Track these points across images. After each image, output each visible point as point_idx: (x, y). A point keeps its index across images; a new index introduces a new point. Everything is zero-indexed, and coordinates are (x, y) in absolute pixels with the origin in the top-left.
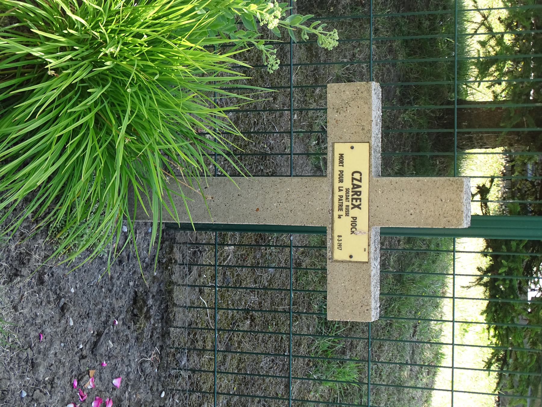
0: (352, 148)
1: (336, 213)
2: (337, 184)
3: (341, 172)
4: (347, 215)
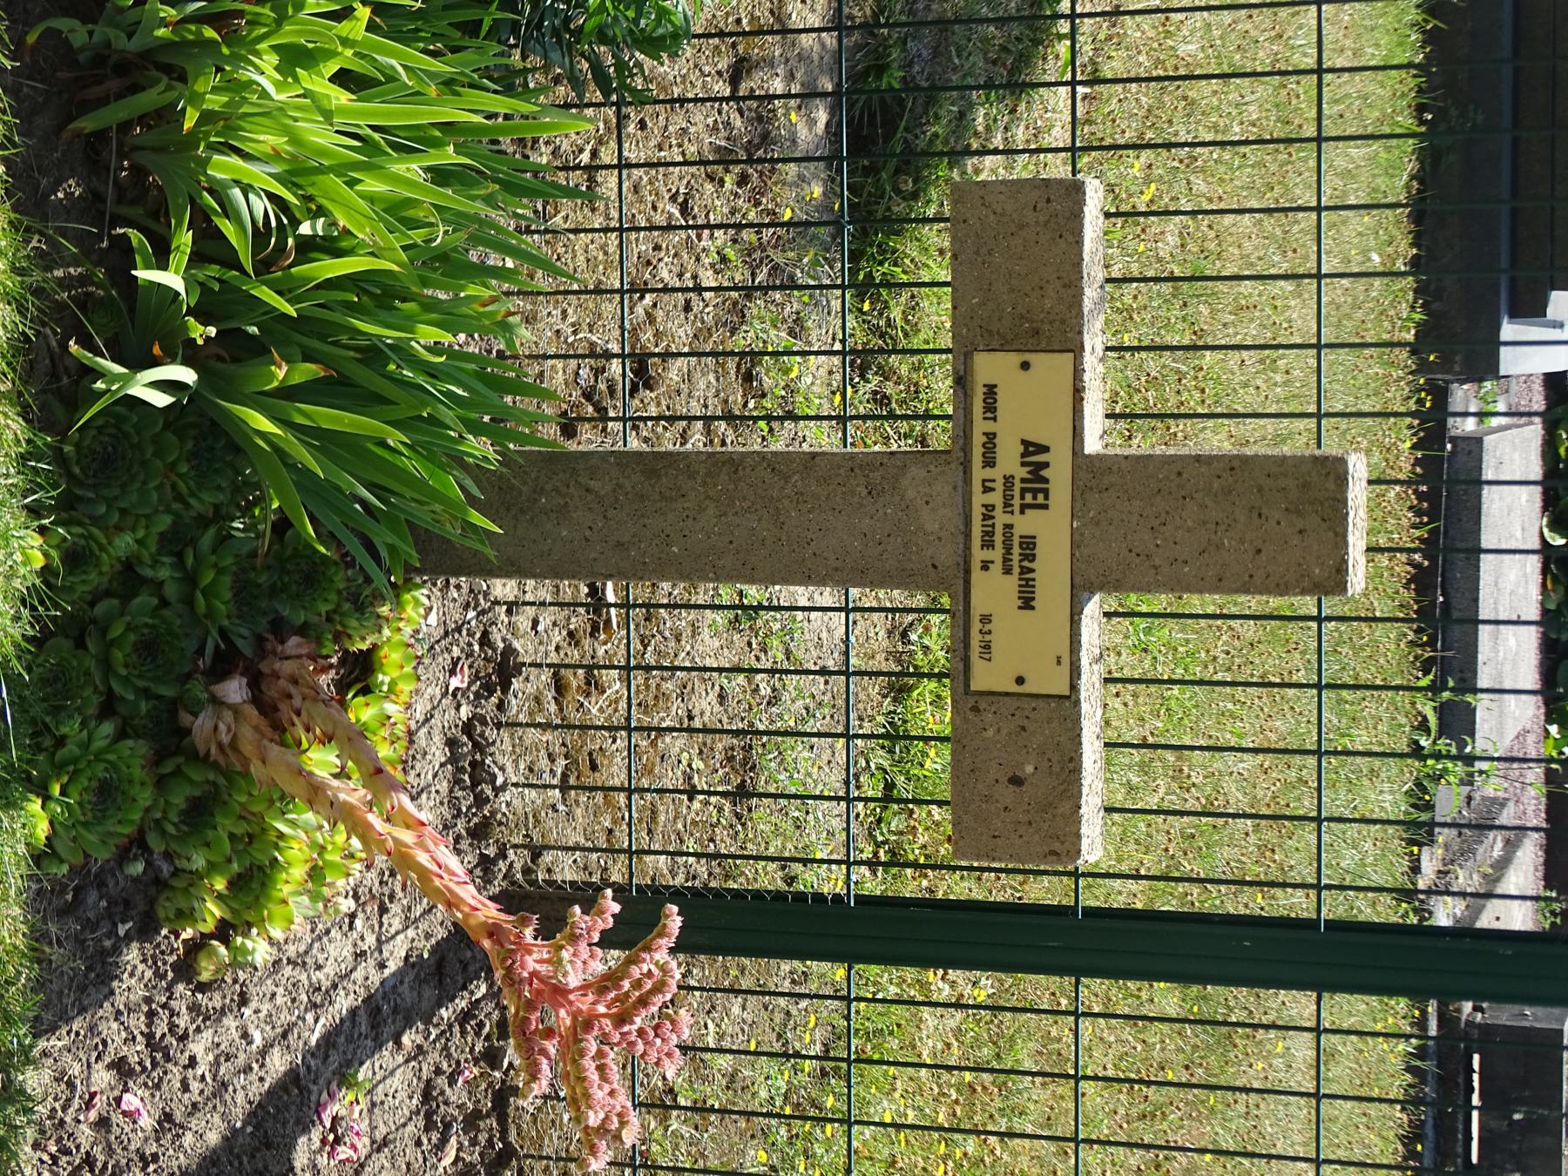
0: (1025, 366)
1: (978, 555)
2: (979, 473)
3: (990, 437)
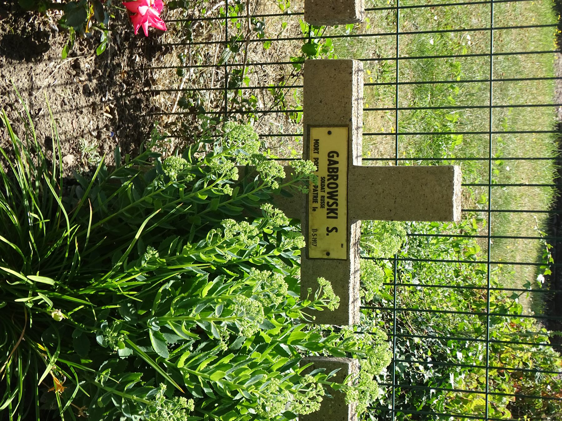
1: (312, 205)
4: (322, 207)
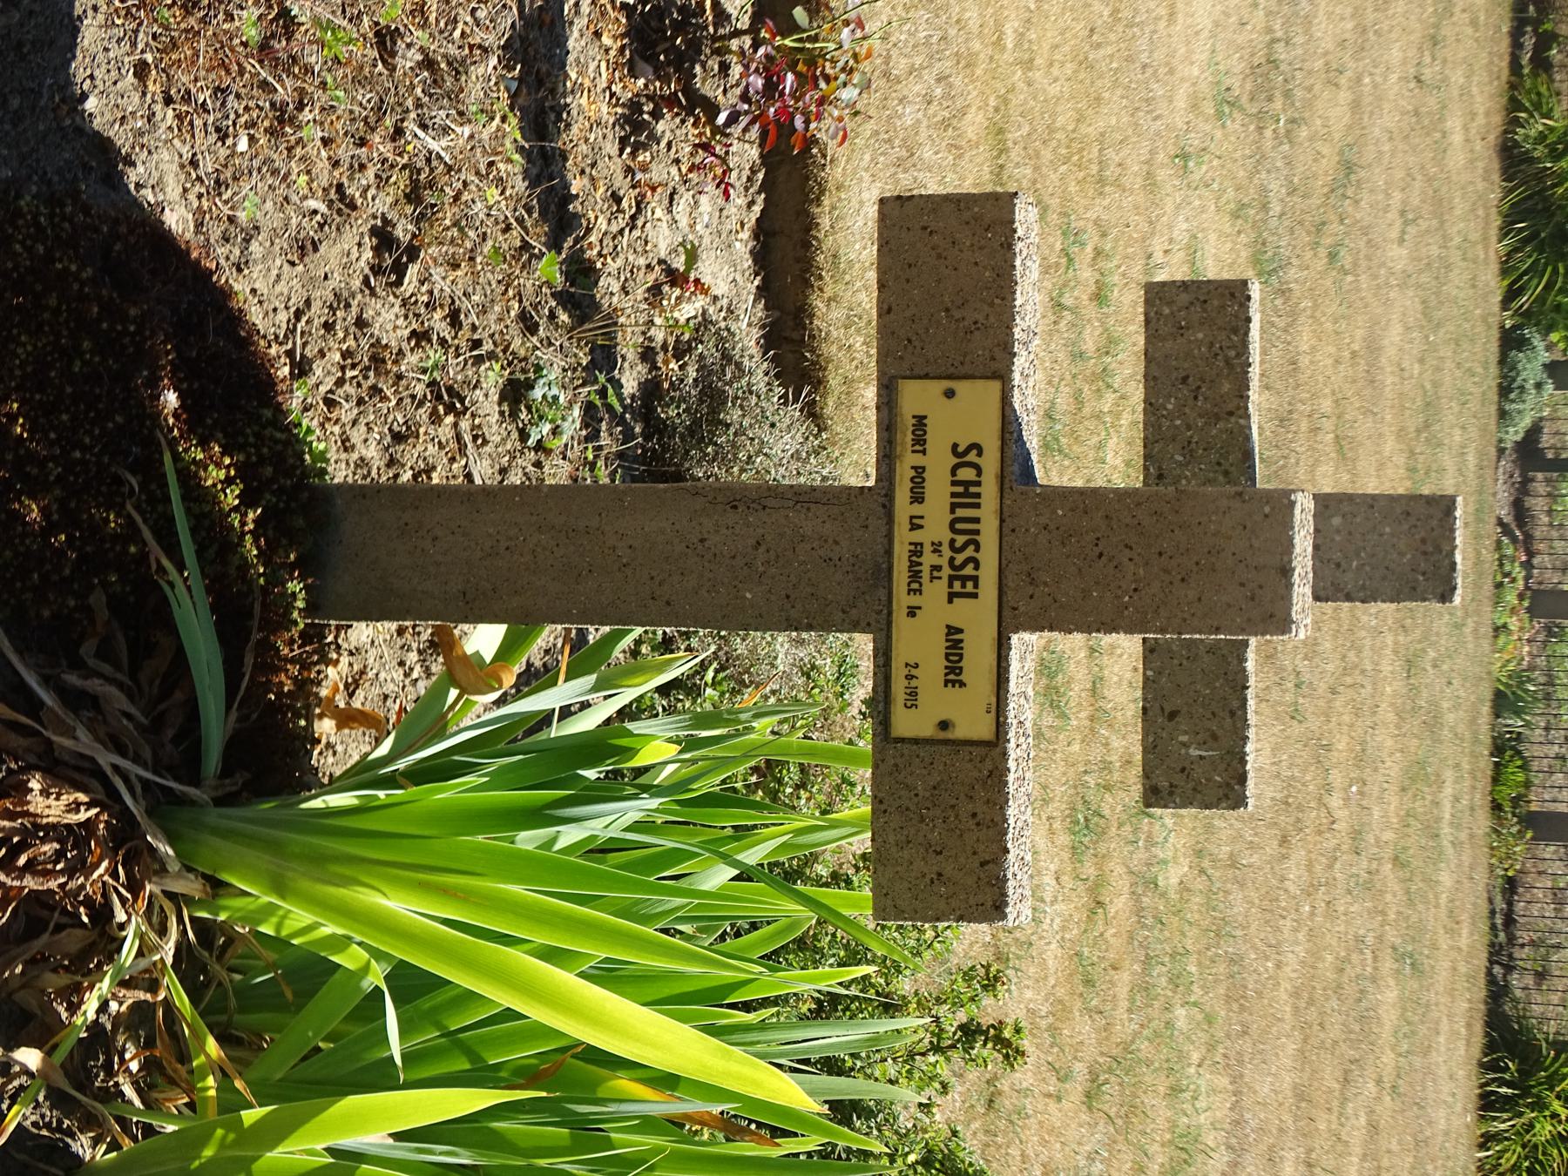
3: (919, 471)
